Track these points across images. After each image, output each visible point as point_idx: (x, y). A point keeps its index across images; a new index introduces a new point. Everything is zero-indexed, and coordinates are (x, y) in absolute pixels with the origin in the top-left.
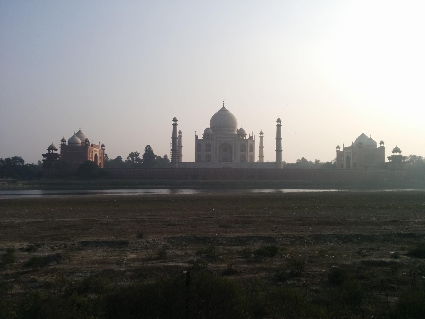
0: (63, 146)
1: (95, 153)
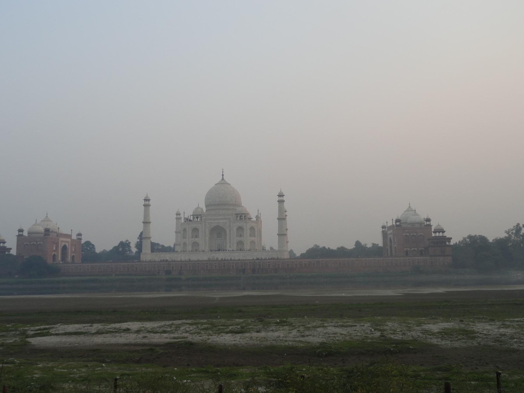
0: (20, 237)
1: (63, 244)
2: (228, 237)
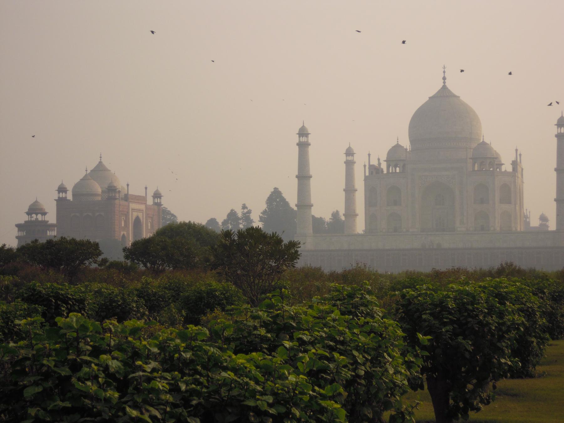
0: (61, 202)
1: (135, 214)
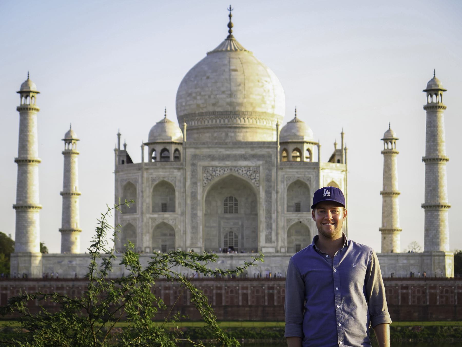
2: (262, 213)
